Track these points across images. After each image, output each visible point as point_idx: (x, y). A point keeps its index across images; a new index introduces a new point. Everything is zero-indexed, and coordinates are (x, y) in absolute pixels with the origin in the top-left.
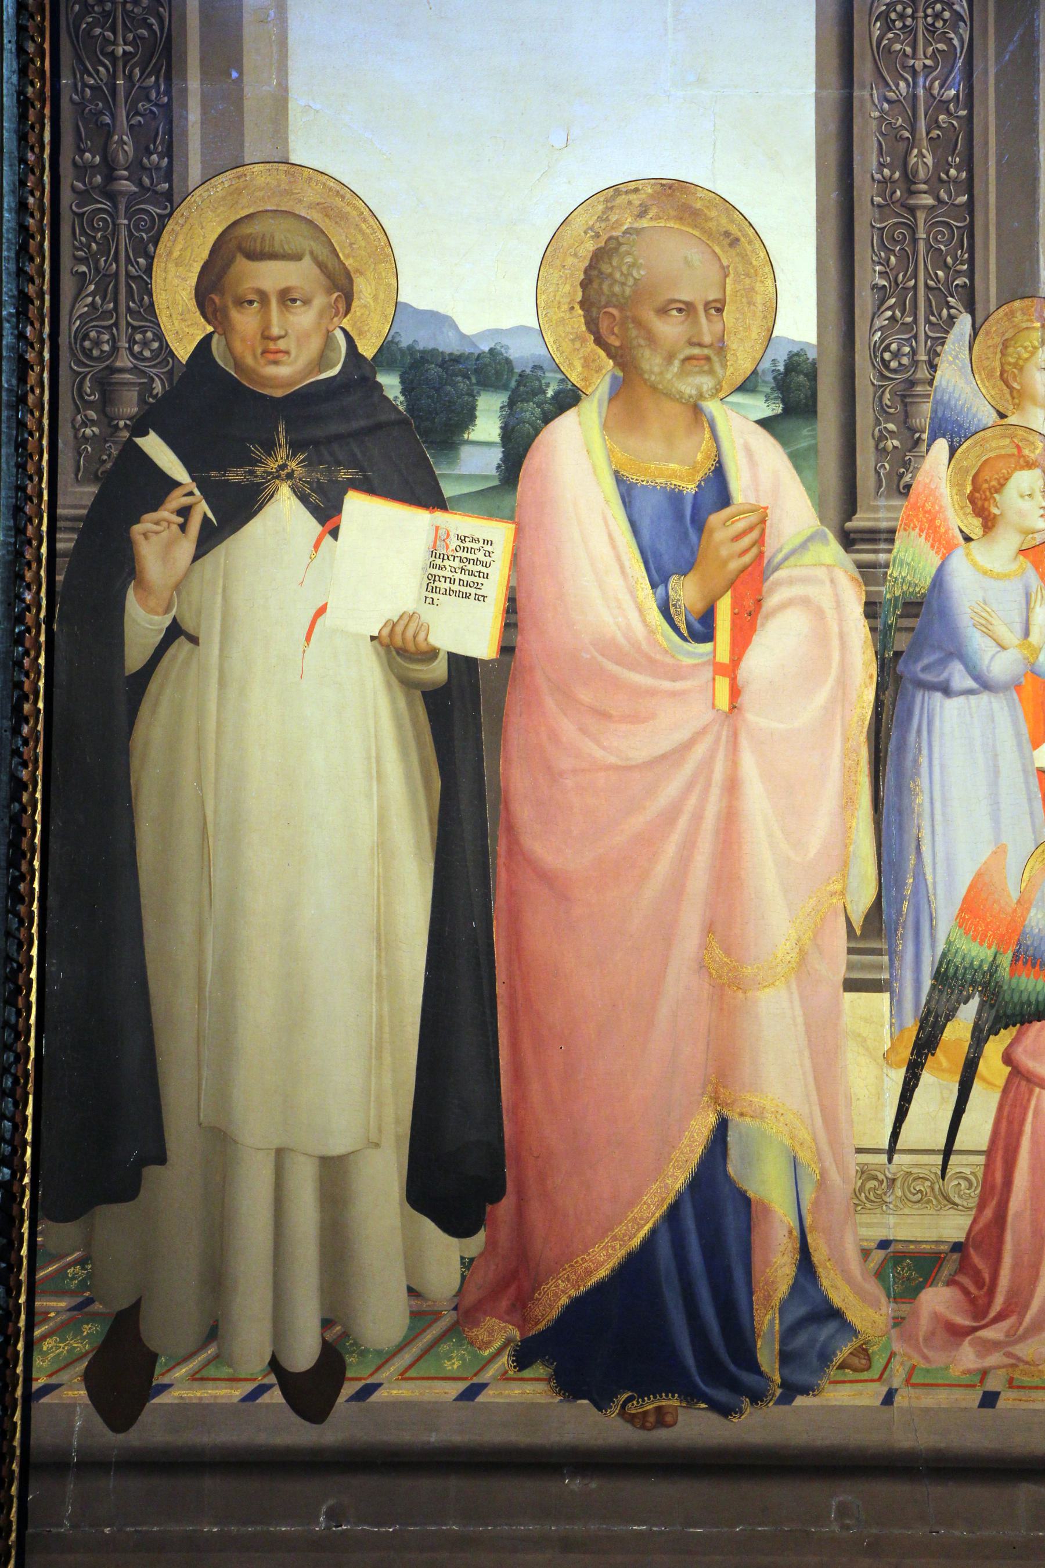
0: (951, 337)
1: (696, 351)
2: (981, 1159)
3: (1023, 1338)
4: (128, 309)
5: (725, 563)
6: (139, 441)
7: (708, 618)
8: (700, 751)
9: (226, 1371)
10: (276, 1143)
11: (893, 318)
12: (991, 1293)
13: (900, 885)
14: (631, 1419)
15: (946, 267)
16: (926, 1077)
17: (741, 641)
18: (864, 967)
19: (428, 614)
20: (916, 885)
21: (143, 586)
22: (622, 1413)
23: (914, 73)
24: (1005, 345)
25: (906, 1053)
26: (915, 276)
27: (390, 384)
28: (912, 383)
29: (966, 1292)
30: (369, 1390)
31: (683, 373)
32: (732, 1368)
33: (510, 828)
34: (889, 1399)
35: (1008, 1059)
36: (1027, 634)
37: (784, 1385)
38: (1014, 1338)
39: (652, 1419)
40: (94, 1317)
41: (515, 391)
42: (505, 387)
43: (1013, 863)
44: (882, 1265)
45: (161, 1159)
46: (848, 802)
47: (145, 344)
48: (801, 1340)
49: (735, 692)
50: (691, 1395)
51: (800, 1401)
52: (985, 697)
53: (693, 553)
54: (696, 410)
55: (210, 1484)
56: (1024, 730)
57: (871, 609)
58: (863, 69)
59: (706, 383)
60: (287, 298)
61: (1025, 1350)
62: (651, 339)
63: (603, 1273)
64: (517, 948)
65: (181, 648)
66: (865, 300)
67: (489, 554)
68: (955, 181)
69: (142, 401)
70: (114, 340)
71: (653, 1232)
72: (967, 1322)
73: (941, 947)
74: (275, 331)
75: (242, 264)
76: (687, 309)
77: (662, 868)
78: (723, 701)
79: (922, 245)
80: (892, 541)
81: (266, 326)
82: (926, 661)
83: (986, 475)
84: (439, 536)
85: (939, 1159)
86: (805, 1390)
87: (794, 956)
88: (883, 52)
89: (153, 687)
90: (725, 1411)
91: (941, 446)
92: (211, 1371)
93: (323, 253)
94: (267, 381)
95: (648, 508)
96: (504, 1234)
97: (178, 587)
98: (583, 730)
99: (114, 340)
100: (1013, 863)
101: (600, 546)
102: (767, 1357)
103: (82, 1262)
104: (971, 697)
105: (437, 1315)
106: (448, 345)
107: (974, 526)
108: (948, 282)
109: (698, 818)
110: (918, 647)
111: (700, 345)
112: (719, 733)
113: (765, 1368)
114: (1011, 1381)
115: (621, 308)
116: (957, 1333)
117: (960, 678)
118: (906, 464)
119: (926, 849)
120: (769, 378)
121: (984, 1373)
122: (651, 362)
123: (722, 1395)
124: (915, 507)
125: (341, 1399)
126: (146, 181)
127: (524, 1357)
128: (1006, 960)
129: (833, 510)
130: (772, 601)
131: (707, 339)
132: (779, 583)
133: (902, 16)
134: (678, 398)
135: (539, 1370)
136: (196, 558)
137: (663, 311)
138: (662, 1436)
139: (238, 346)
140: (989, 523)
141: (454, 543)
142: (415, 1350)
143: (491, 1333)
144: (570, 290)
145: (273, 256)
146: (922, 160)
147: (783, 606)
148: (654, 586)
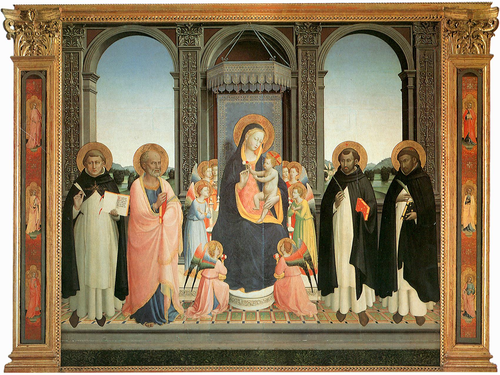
0: (194, 167)
1: (157, 169)
2: (197, 289)
3: (202, 314)
4: (73, 165)
5: (161, 201)
6: (74, 184)
7: (158, 209)
8: (157, 229)
9: (89, 320)
10: (95, 287)
11: (186, 164)
12: (198, 308)
13: (186, 248)
14: (147, 326)
15: (194, 156)
16: (189, 277)
17: (163, 214)
18: (181, 261)
19: (117, 210)
20: (188, 250)
21: (75, 206)
22: (145, 325)
23: (189, 127)
24: (202, 168)
25: (187, 274)
26: (189, 157)
27: (111, 175)
28: (188, 174)
29: (194, 307)
30: (109, 322)
31: (155, 173)
32: (161, 319)
33: (129, 241)
34: (183, 323)
35: (201, 274)
36: (205, 212)
37: (168, 321)
38: (201, 314)
39: (150, 326)
40: (70, 312)
41: (130, 176)
42: (128, 175)
43: (203, 245)
44: (183, 304)
45: (79, 290)
46: (179, 237)
47: (75, 170)
48: (170, 315)
49: (162, 221)
50: (155, 323)
51: (171, 323)
52: (199, 221)
53: (156, 200)
54: (157, 178)
55: (87, 335)
56: (205, 226)
57: (182, 208)
58: (181, 127)
59: (158, 174)
60: (96, 162)
61: (202, 316)
62: (150, 168)
63: (143, 305)
64: (130, 259)
65: (81, 215)
66: (182, 161)
67: (126, 200)
68: (195, 143)
69: (75, 178)
70: (71, 169)
71: (150, 300)
72: (195, 312)
73: (192, 258)
74: (95, 167)
75: (89, 157)
76: (156, 163)
77: (152, 247)
78: (161, 222)
79: (190, 153)
80: (185, 198)
81: (93, 166)
82: (190, 216)
83: (199, 188)
84: (119, 198)
85: (191, 289)
86: (171, 322)
87: (170, 259)
88: (184, 124)
89: (77, 221)
90: (160, 325)
91: (193, 183)
92: (87, 319)
93: (102, 156)
94: (94, 175)
95: (150, 192)
96: (128, 300)
97: (80, 206)
98: (140, 227)
99: (71, 169)
100: (203, 245)
101: (143, 199)
102: (166, 317)
103: (68, 304)
104: (197, 221)
105: (119, 312)
106: (120, 169)
107: (198, 196)
108: (194, 159)
109: (157, 239)
110: (189, 214)
111: (157, 168)
112: (160, 228)
113: (166, 319)
114: (201, 320)
115: (146, 163)
116: (193, 313)
117: (195, 218)
118: (188, 186)
119: (190, 244)
120: (167, 173)
121: (197, 319)
122: (150, 171)
123: (160, 323)
124: (189, 193)
125: (105, 323)
126: (76, 145)
127: (131, 318)
128: (201, 260)
129: (177, 193)
130: (167, 207)
131: (158, 168)
132: (169, 204)
133: (187, 119)
134: (154, 177)
135: (134, 319)
136: (83, 201)
137: (152, 163)
138: (151, 328)
139: (89, 170)
140: (200, 195)
141: (121, 199)
142: (116, 316)
143: (127, 314)
144: (138, 160)
145: (94, 156)
146: (190, 140)
147: (170, 208)
148: (150, 205)
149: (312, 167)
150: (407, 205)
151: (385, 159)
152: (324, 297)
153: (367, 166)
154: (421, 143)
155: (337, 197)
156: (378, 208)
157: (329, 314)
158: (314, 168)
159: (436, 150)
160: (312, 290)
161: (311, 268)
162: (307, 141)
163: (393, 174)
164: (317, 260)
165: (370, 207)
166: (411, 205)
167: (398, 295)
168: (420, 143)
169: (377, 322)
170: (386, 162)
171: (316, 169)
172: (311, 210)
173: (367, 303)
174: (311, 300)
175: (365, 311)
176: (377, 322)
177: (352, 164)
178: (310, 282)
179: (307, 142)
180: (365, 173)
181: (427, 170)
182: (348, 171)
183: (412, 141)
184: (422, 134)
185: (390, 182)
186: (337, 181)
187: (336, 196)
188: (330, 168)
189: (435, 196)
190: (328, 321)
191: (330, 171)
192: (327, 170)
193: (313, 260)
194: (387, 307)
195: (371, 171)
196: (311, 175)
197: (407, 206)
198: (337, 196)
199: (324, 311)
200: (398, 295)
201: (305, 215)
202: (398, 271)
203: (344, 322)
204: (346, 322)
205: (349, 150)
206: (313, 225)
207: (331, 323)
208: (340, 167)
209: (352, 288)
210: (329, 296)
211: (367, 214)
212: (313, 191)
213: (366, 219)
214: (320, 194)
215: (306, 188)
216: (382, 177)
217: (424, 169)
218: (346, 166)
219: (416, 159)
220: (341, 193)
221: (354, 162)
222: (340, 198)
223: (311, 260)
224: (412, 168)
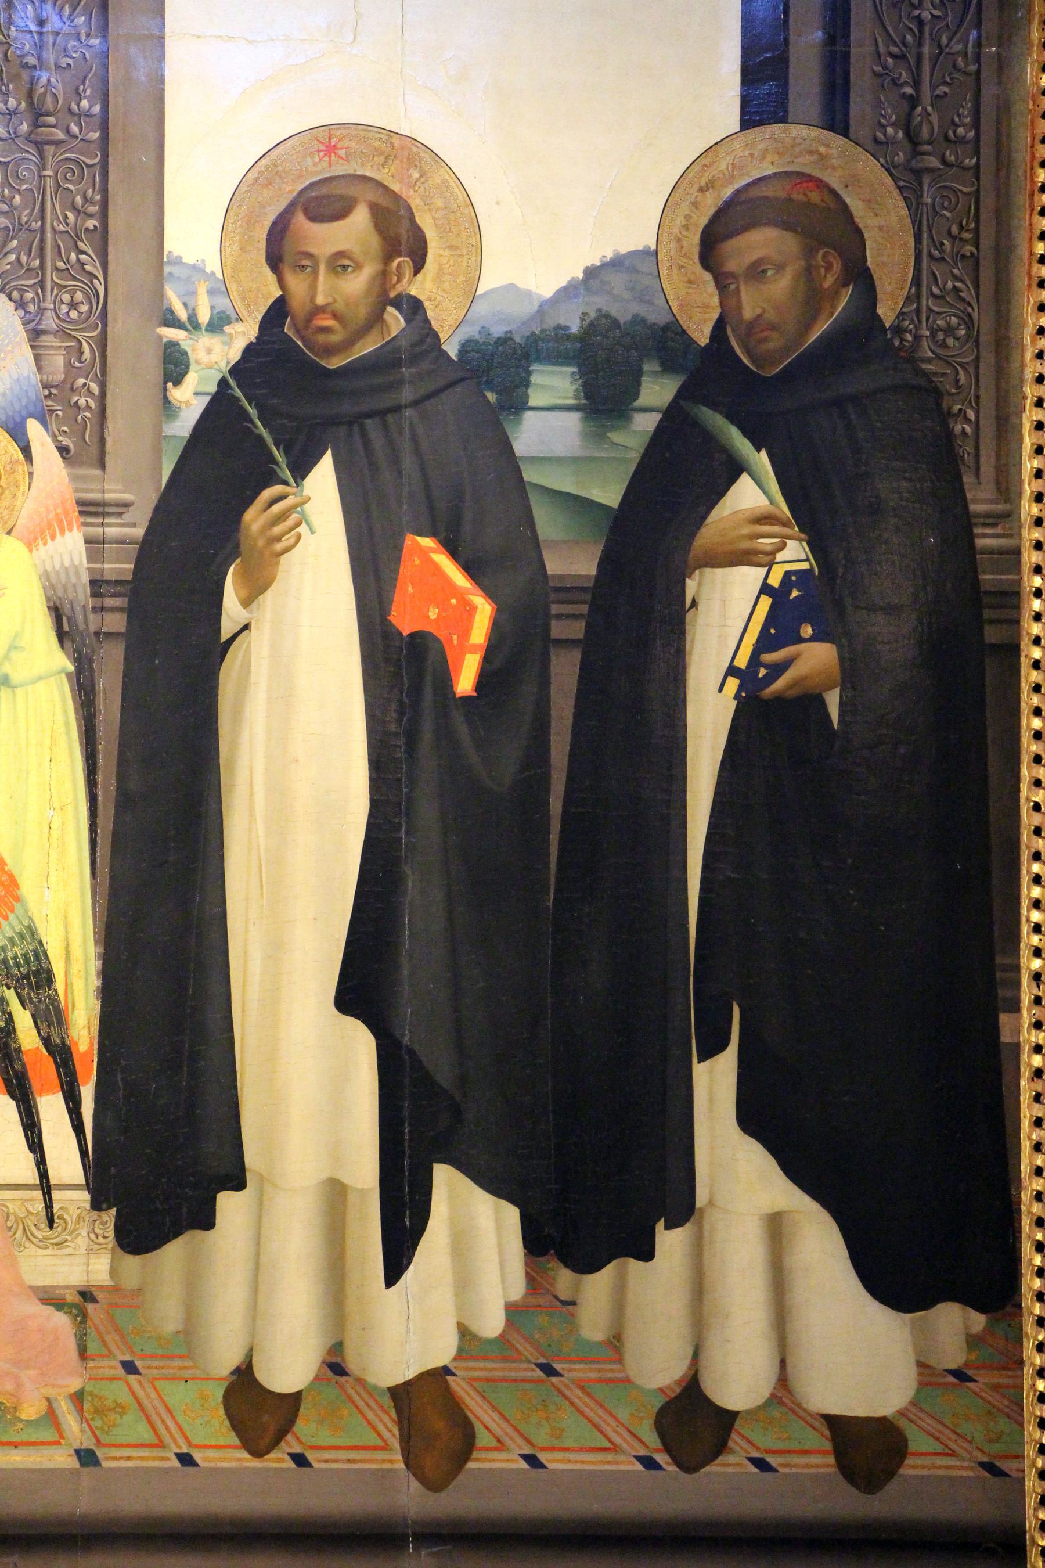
149: (73, 305)
150: (766, 589)
151: (609, 255)
152: (132, 1262)
153: (481, 309)
154: (878, 147)
155: (255, 527)
156: (554, 609)
157: (178, 1395)
158: (84, 308)
159: (988, 201)
160: (49, 1206)
161: (47, 1042)
162: (37, 115)
163: (669, 367)
164: (96, 982)
165: (490, 594)
166: (795, 593)
167: (698, 1250)
168: (870, 146)
169: (532, 1460)
170: (617, 281)
171: (104, 315)
172: (57, 612)
173: (460, 1307)
174: (40, 1282)
175: (446, 1371)
176: (532, 1460)
177: (368, 292)
178: (35, 1144)
179: (36, 125)
180: (465, 348)
181: (917, 338)
182: (335, 338)
183: (814, 132)
184: (884, 78)
185: (646, 423)
186: (252, 411)
187: (249, 515)
188: (204, 318)
189: (977, 530)
190: (160, 1445)
191: (205, 340)
192: (175, 323)
193: (59, 985)
194: (615, 1343)
195: (506, 340)
196: (57, 361)
197: (766, 602)
198: (254, 518)
199: (130, 1368)
200: (698, 1250)
201: (13, 647)
202: (700, 1071)
203: (278, 1459)
204: (300, 1460)
205: (352, 190)
206: (67, 724)
207: (186, 1460)
208: (278, 312)
209: (351, 1198)
210: (173, 1252)
211: (473, 649)
212: (73, 478)
213: (465, 682)
214: (127, 497)
215: (26, 451)
216: (585, 386)
217: (898, 330)
218: (320, 300)
219: (837, 266)
220: (282, 497)
221: (384, 274)
222: (277, 530)
223: (50, 980)
224: (808, 327)
